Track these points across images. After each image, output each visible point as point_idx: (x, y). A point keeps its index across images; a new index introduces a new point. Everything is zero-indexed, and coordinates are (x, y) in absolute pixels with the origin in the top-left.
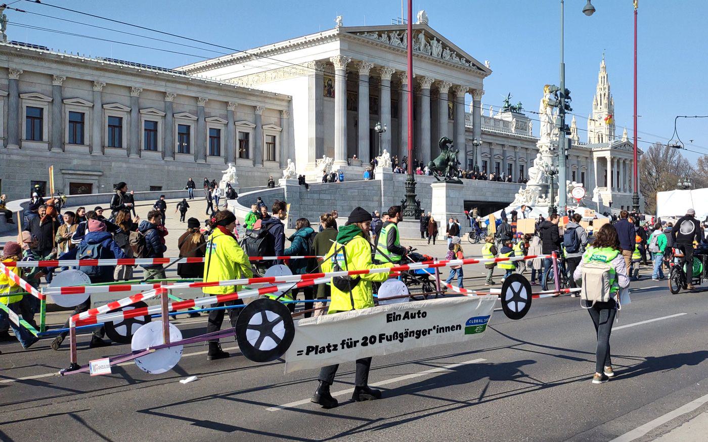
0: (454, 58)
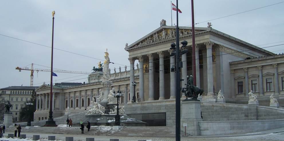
0: (184, 33)
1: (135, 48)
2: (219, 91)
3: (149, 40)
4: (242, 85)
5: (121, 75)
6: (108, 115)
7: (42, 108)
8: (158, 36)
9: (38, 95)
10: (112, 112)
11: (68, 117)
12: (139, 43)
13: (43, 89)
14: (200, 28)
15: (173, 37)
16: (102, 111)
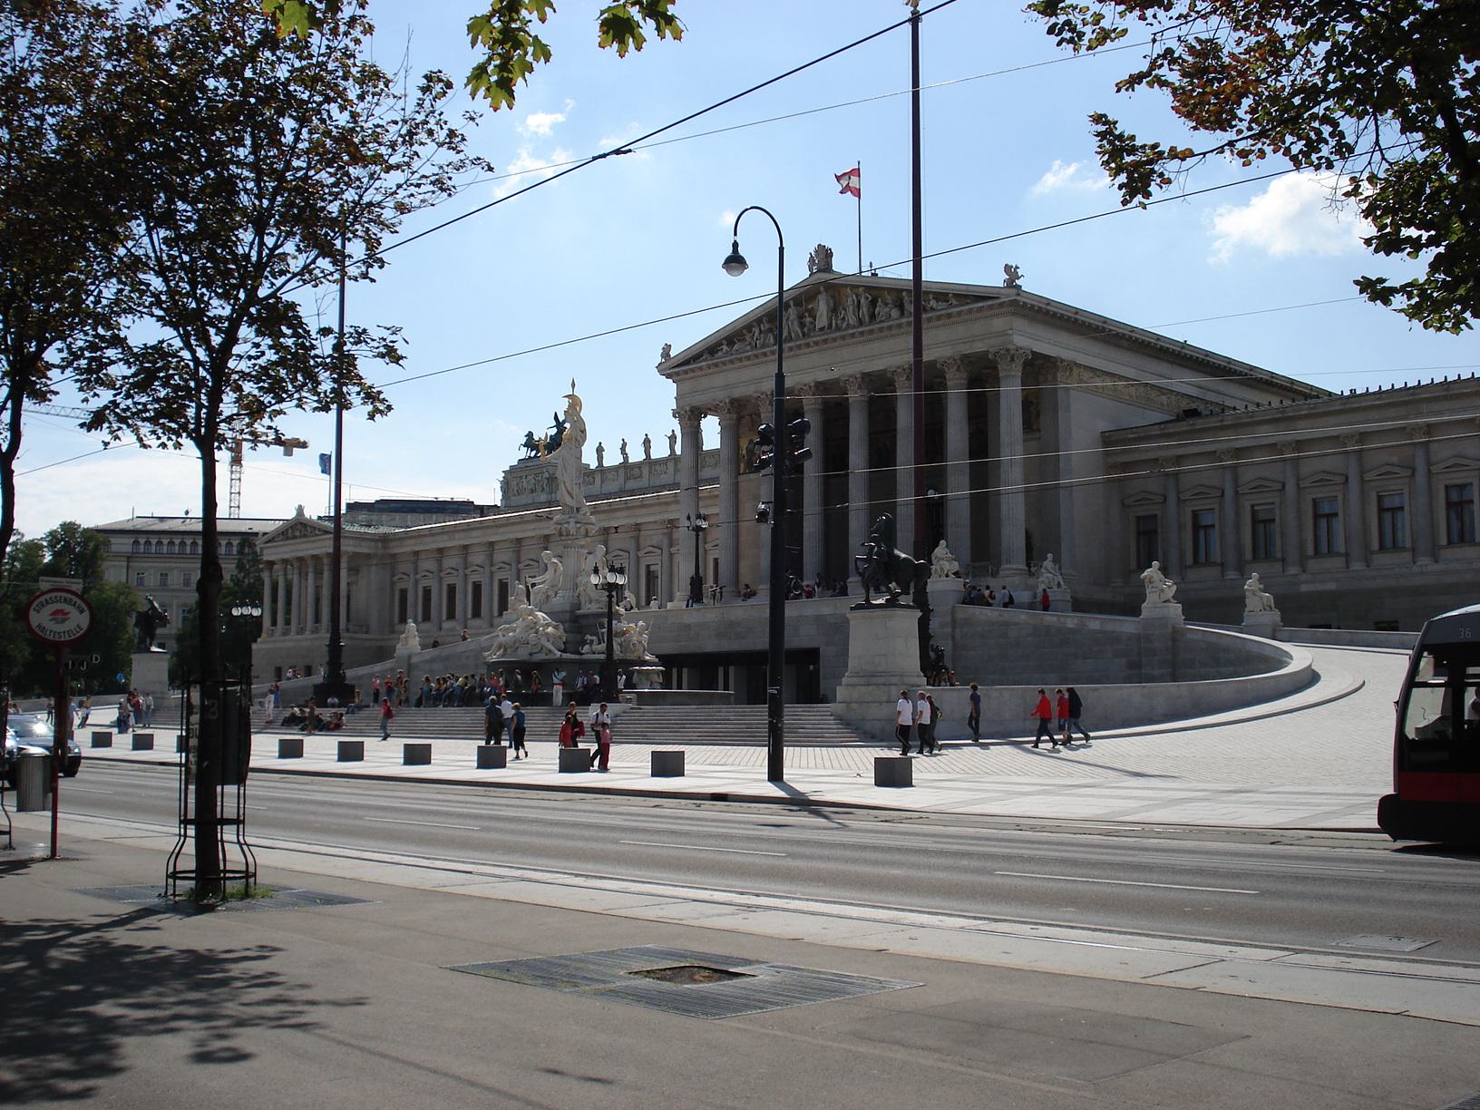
1: (701, 369)
2: (1046, 559)
3: (761, 332)
4: (1155, 532)
5: (650, 473)
6: (577, 657)
7: (288, 622)
8: (801, 317)
9: (271, 564)
10: (595, 647)
11: (409, 665)
12: (719, 344)
13: (294, 537)
14: (970, 288)
15: (861, 323)
16: (553, 644)
